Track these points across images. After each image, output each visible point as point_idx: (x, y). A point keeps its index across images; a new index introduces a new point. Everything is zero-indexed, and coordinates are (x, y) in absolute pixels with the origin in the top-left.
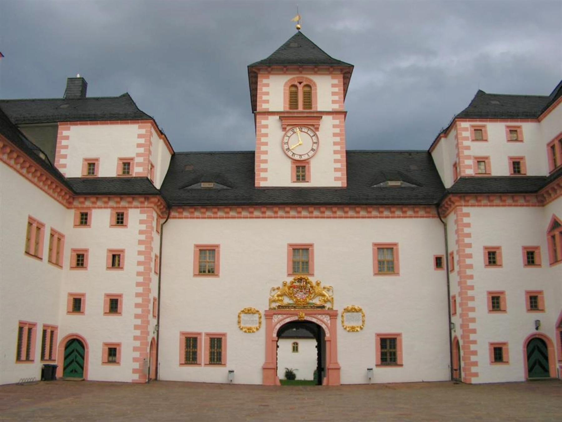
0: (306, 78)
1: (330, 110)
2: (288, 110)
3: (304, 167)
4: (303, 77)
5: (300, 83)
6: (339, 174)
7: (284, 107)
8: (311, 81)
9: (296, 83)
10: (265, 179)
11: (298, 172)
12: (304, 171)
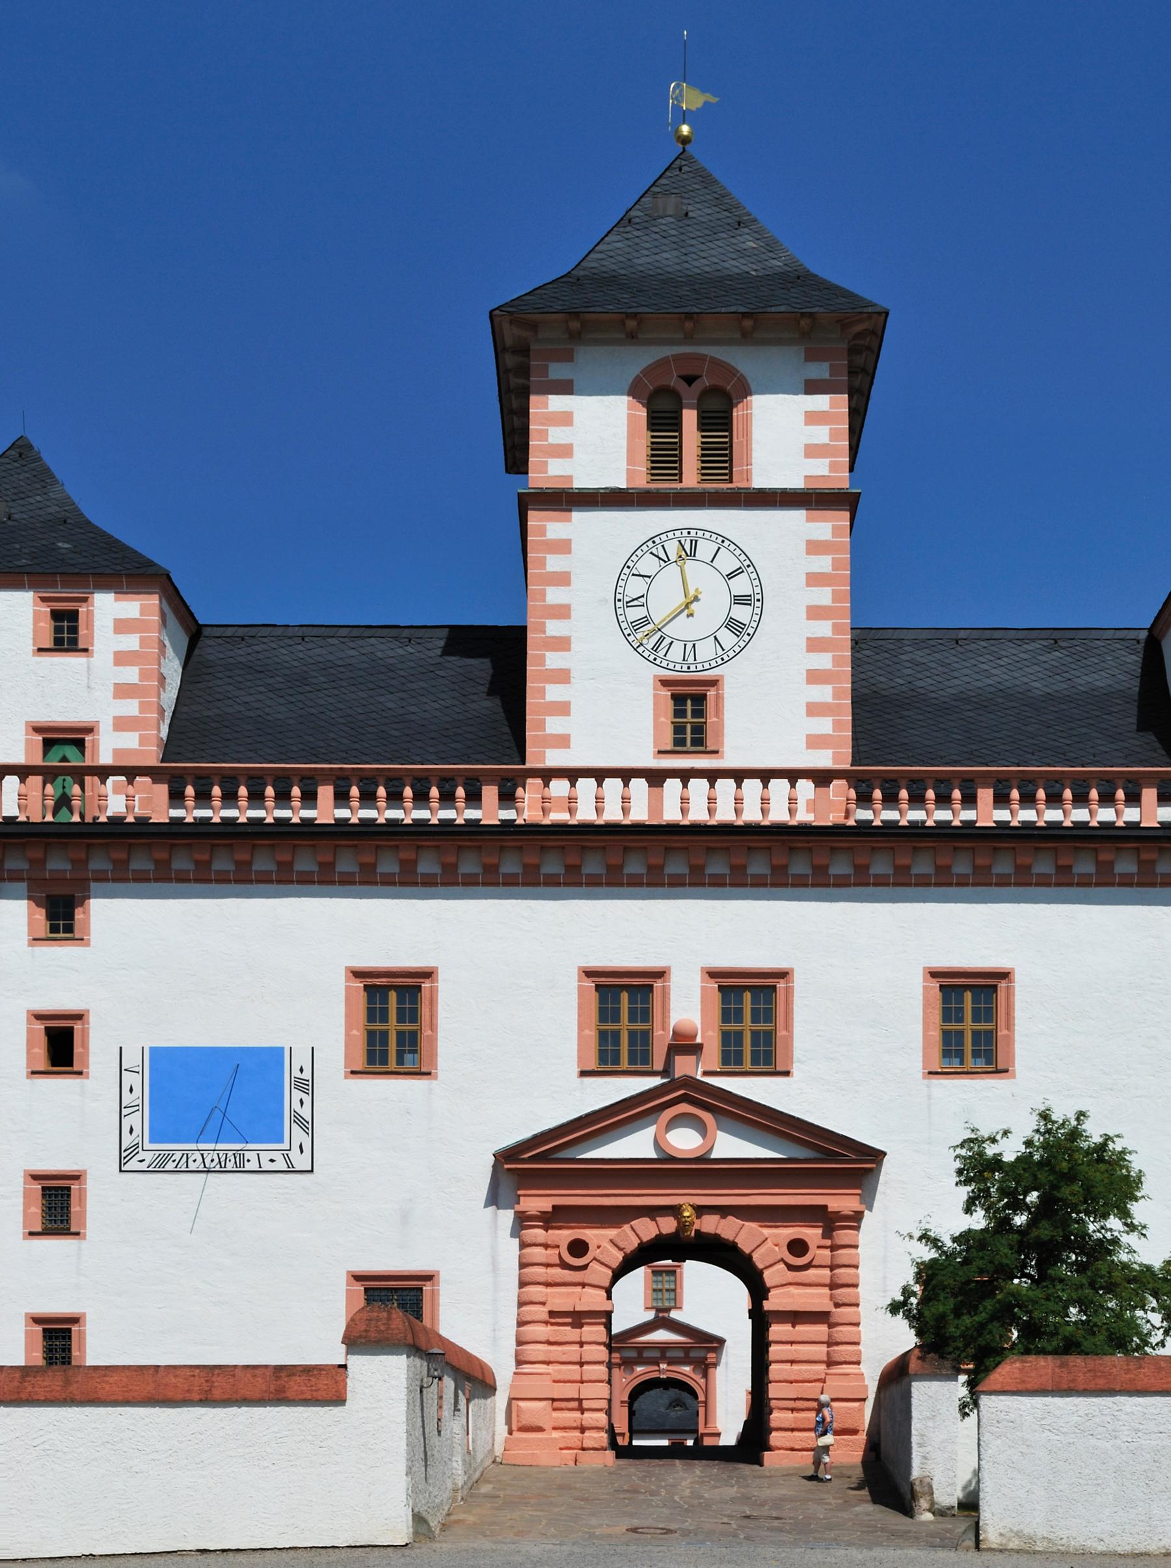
0: (717, 363)
1: (794, 481)
2: (642, 482)
3: (700, 699)
4: (702, 358)
5: (690, 380)
6: (824, 725)
7: (630, 474)
8: (731, 371)
9: (674, 382)
10: (563, 741)
11: (680, 713)
12: (699, 713)
